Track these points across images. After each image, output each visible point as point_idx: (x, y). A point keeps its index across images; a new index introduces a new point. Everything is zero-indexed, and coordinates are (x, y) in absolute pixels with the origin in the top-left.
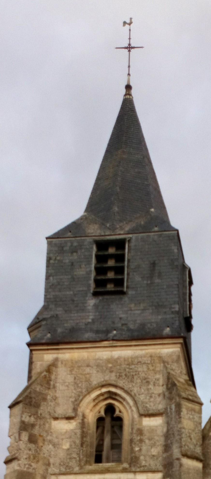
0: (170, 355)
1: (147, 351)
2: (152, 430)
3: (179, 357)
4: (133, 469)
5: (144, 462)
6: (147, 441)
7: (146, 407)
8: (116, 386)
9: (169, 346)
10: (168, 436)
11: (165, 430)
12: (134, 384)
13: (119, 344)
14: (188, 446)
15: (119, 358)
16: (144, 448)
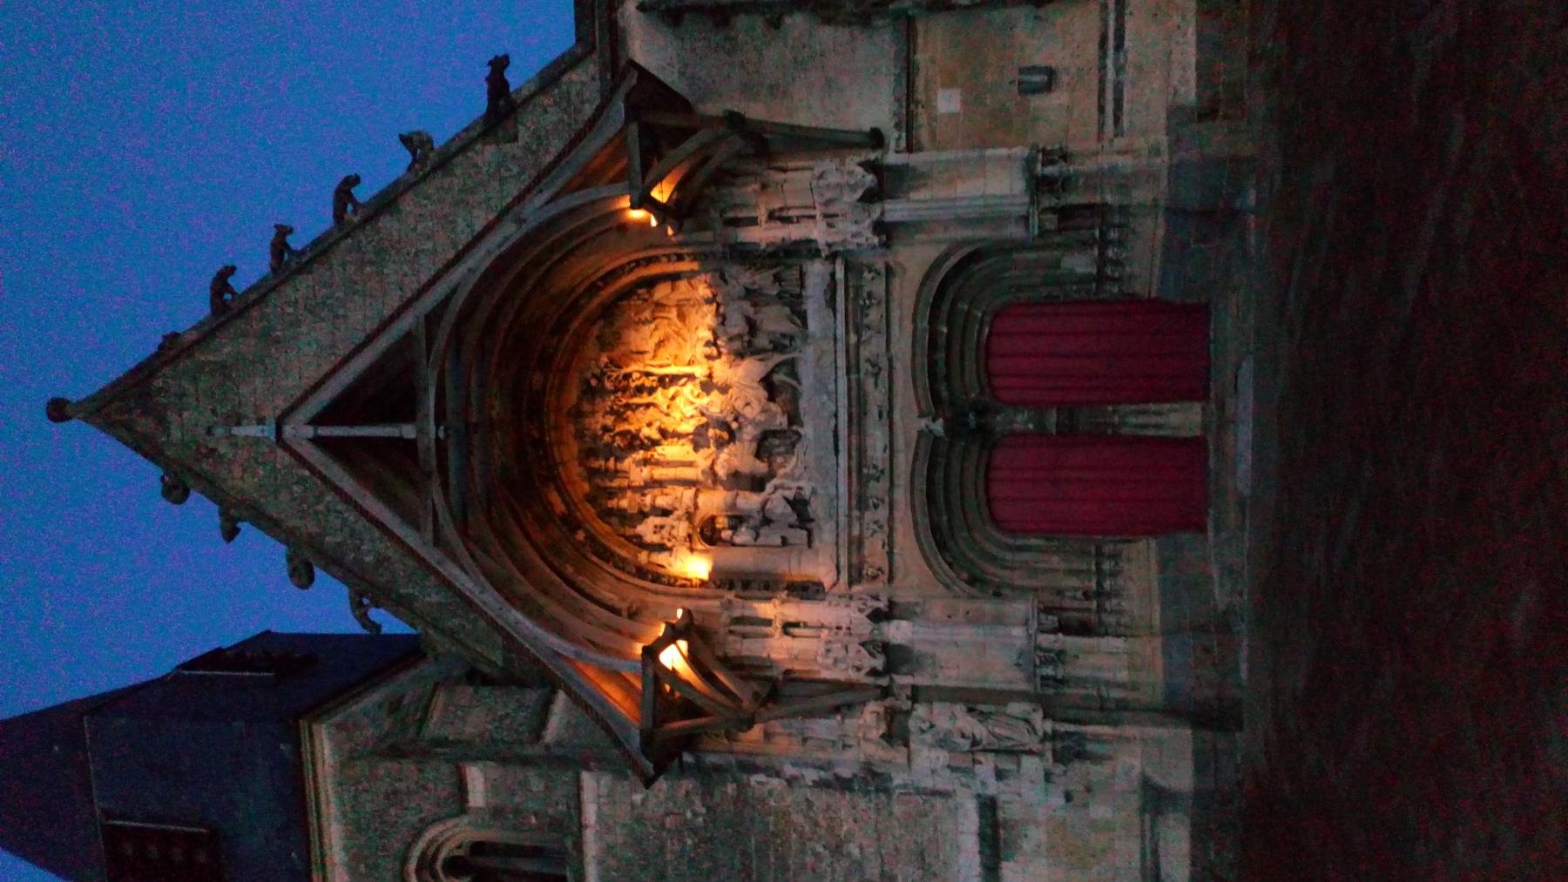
0: (338, 748)
1: (330, 792)
2: (493, 788)
3: (340, 727)
4: (575, 829)
5: (560, 808)
6: (517, 799)
7: (446, 799)
8: (405, 860)
9: (317, 743)
10: (504, 761)
11: (492, 763)
12: (400, 821)
13: (316, 851)
14: (521, 725)
15: (345, 849)
16: (531, 805)
